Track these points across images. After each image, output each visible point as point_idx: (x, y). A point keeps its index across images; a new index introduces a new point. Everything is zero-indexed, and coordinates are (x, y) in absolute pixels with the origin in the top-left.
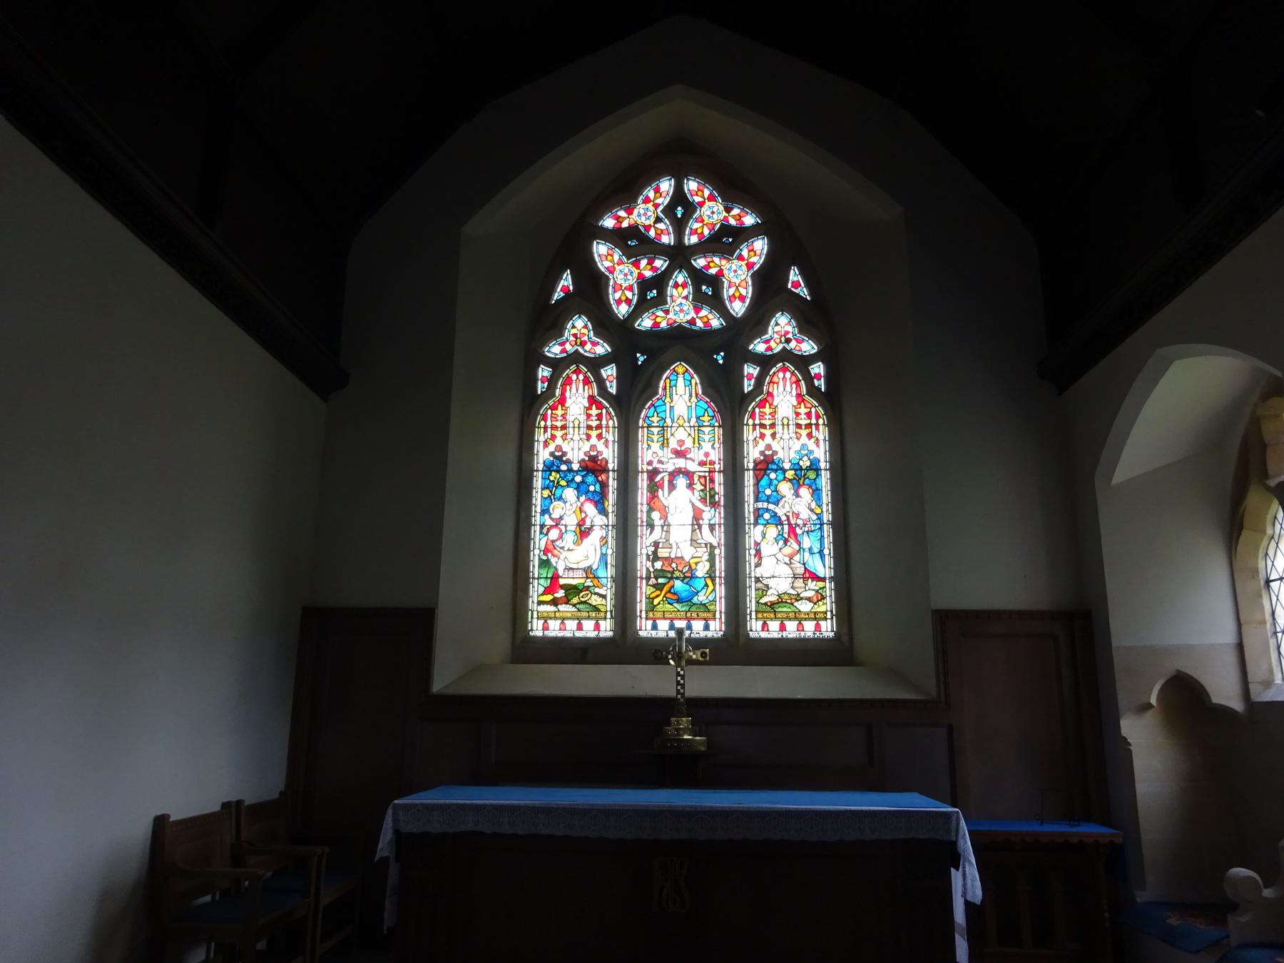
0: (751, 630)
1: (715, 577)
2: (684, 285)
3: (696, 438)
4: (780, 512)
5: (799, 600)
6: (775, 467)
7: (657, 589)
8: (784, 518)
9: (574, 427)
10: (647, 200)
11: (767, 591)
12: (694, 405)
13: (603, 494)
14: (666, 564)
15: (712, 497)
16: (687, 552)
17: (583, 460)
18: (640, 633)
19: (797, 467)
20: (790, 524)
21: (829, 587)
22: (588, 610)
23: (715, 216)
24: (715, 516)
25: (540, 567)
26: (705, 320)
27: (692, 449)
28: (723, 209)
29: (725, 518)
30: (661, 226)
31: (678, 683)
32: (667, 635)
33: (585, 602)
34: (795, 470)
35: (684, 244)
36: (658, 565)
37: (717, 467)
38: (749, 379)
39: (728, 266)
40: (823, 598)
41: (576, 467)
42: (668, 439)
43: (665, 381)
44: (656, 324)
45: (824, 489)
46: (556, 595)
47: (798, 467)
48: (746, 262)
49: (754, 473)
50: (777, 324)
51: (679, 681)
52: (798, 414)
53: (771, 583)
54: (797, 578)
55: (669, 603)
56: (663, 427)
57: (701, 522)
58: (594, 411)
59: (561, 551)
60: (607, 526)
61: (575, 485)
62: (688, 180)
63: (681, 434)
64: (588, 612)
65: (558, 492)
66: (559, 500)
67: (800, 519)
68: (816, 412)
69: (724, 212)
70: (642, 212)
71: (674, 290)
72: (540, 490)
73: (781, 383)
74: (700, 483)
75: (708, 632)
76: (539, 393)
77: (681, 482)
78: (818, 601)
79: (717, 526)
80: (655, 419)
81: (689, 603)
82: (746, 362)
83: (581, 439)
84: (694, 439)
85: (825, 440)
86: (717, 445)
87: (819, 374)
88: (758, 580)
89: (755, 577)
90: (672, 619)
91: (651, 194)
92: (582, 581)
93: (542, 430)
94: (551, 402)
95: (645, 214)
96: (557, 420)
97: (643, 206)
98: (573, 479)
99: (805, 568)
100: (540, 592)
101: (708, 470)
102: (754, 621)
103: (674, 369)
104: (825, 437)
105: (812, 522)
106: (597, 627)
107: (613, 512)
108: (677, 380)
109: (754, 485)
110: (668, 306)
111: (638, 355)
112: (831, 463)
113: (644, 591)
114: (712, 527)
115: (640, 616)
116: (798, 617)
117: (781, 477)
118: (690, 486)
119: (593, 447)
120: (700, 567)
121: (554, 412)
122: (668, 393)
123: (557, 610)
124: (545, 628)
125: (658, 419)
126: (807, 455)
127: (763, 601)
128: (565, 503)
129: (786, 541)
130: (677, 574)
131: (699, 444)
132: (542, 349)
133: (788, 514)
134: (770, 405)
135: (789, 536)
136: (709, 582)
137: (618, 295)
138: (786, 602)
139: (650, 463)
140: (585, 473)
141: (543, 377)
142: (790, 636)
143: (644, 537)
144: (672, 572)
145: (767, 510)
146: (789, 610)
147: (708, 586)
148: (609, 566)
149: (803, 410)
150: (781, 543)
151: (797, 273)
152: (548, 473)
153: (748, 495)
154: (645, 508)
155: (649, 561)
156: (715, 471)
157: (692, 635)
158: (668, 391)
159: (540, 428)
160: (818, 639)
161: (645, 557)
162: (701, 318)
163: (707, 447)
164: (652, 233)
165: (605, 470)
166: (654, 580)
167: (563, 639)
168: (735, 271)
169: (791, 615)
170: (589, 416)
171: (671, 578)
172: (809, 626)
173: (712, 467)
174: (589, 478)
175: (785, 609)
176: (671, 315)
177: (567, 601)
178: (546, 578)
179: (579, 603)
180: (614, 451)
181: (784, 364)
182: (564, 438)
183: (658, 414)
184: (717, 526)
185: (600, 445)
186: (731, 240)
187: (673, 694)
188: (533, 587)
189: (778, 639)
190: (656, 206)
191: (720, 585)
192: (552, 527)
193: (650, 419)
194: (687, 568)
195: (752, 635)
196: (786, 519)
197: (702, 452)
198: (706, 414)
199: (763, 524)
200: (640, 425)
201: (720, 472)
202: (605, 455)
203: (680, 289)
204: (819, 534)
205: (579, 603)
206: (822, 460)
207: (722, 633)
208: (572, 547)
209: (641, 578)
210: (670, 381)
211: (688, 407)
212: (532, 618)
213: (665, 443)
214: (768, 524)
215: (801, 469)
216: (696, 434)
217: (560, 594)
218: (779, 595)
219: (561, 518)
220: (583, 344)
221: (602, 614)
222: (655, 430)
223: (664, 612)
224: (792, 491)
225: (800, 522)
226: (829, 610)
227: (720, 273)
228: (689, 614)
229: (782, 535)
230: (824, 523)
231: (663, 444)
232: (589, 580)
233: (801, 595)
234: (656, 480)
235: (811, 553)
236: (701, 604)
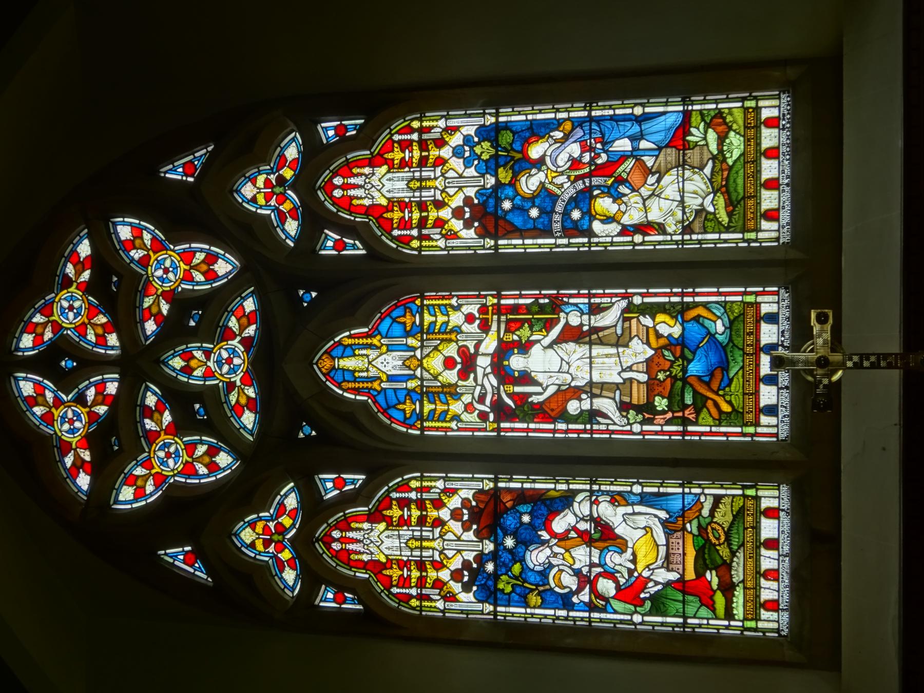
0: (777, 239)
1: (682, 303)
2: (188, 356)
3: (441, 336)
4: (569, 191)
5: (724, 156)
6: (492, 202)
7: (704, 406)
8: (580, 185)
9: (422, 548)
10: (48, 418)
11: (708, 213)
12: (384, 341)
13: (536, 499)
14: (661, 389)
15: (542, 309)
16: (639, 351)
17: (477, 533)
18: (782, 436)
19: (492, 164)
20: (590, 175)
22: (741, 529)
23: (77, 304)
24: (576, 305)
25: (664, 614)
26: (244, 320)
27: (461, 344)
28: (65, 291)
29: (579, 288)
30: (91, 393)
31: (873, 366)
32: (787, 388)
33: (728, 535)
34: (498, 166)
35: (118, 356)
36: (661, 403)
37: (492, 301)
38: (344, 246)
39: (157, 284)
40: (720, 114)
41: (489, 547)
42: (443, 386)
43: (344, 390)
44: (251, 404)
45: (530, 117)
46: (715, 586)
47: (493, 162)
48: (151, 253)
49: (503, 238)
50: (254, 200)
51: (872, 363)
52: (404, 164)
53: (693, 203)
54: (684, 161)
55: (729, 385)
56: (422, 394)
57: (586, 328)
58: (395, 512)
59: (636, 574)
60: (592, 492)
61: (520, 549)
62: (18, 349)
63: (435, 363)
64: (745, 529)
65: (532, 578)
66: (547, 577)
67: (581, 156)
68: (398, 132)
69: (70, 290)
70: (66, 427)
71: (195, 373)
72: (529, 611)
73: (352, 192)
74: (518, 329)
75: (781, 316)
76: (360, 607)
77: (516, 362)
78: (725, 123)
79: (592, 301)
80: (408, 407)
81: (729, 349)
82: (314, 252)
83: (441, 536)
84: (442, 340)
85: (447, 118)
86: (454, 302)
87: (336, 128)
88: (687, 229)
89: (683, 233)
90: (759, 380)
91: (38, 410)
92: (689, 539)
93: (426, 603)
94: (379, 587)
95: (71, 422)
96: (409, 577)
97: (57, 425)
98: (510, 551)
99: (667, 146)
100: (709, 614)
101: (495, 317)
102: (761, 235)
103: (324, 374)
104: (442, 116)
105: (587, 137)
106: (772, 513)
107: (568, 483)
108: (343, 370)
109: (523, 238)
110: (221, 384)
111: (301, 435)
112: (485, 106)
113: (707, 429)
114: (595, 310)
115: (752, 435)
117: (509, 192)
118: (525, 347)
119: (456, 515)
120: (664, 330)
121: (394, 583)
122: (365, 385)
123: (741, 585)
124: (772, 605)
125: (408, 401)
126: (472, 148)
127: (723, 217)
128: (551, 566)
129: (620, 181)
130: (676, 370)
131: (452, 331)
132: (287, 601)
133: (572, 178)
134: (389, 209)
135: (611, 176)
136: (693, 313)
137: (203, 470)
138: (727, 179)
139: (483, 416)
140: (499, 531)
141: (334, 600)
142: (788, 171)
143: (611, 427)
144: (674, 379)
145: (566, 214)
146: (741, 172)
147: (699, 316)
148: (662, 490)
149: (397, 155)
150: (623, 189)
151: (171, 166)
152: (499, 595)
153: (540, 246)
154: (562, 426)
155: (654, 419)
156: (498, 304)
157: (785, 344)
158: (361, 385)
159: (421, 606)
160: (793, 121)
161: (646, 428)
162: (242, 328)
163: (456, 319)
164: (102, 409)
166: (687, 412)
167: (795, 574)
168: (166, 271)
169: (750, 169)
170: (404, 522)
171: (685, 380)
172: (769, 138)
173: (490, 308)
174: (508, 523)
175: (740, 181)
176: (237, 379)
177: (724, 568)
178: (684, 602)
179: (729, 545)
180: (463, 479)
181: (320, 188)
182: (438, 566)
183: (400, 403)
184: (592, 301)
185: (454, 502)
186: (115, 279)
187: (895, 375)
188: (700, 626)
189: (793, 193)
190: (58, 402)
191: (699, 294)
192: (594, 591)
193: (408, 416)
194: (666, 353)
195: (785, 238)
196: (581, 182)
197: (466, 328)
198: (402, 320)
199: (591, 222)
200: (418, 432)
201: (499, 297)
202: (469, 494)
203: (193, 363)
204: (607, 124)
205: (729, 545)
206: (480, 121)
207: (782, 291)
208: (628, 554)
209: (684, 433)
210: (344, 381)
211: (388, 350)
212: (756, 630)
213: (451, 392)
214: (589, 211)
215: (495, 157)
216: (434, 336)
217: (712, 578)
218: (715, 192)
219: (577, 573)
220: (281, 530)
221: (750, 503)
222: (428, 407)
223: (744, 394)
224: (534, 171)
225: (587, 158)
226: (739, 104)
227: (169, 296)
228: (749, 350)
229: (609, 188)
230: (589, 115)
231: (451, 395)
232: (688, 526)
233: (715, 152)
234: (514, 407)
235: (641, 136)
236: (730, 328)
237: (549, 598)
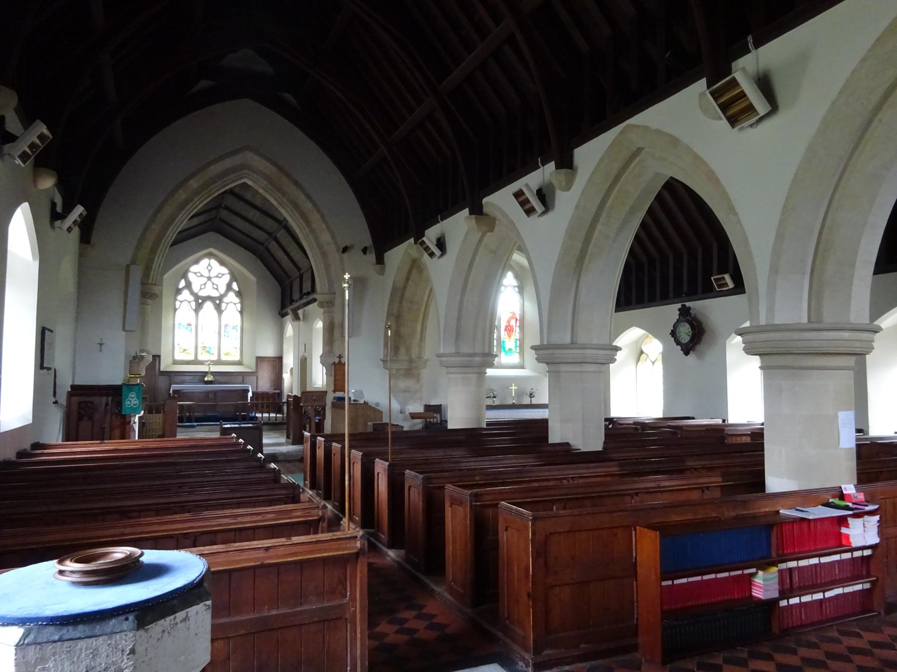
13: (191, 330)
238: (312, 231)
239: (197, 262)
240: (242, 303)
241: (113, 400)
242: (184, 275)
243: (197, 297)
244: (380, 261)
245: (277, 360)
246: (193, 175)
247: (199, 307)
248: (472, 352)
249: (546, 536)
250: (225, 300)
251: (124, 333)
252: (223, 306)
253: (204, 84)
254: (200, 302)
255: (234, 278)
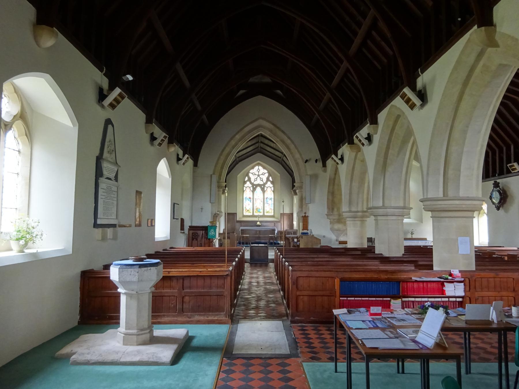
4: (268, 203)
13: (251, 201)
21: (273, 210)
41: (248, 198)
114: (261, 204)
116: (269, 213)
165: (251, 198)
237: (245, 201)
238: (292, 153)
239: (253, 168)
240: (274, 187)
241: (205, 232)
242: (247, 175)
243: (253, 184)
244: (324, 165)
245: (291, 215)
246: (237, 134)
247: (254, 190)
248: (356, 210)
249: (297, 277)
250: (266, 186)
251: (211, 204)
252: (266, 188)
253: (241, 92)
254: (254, 187)
255: (270, 175)
